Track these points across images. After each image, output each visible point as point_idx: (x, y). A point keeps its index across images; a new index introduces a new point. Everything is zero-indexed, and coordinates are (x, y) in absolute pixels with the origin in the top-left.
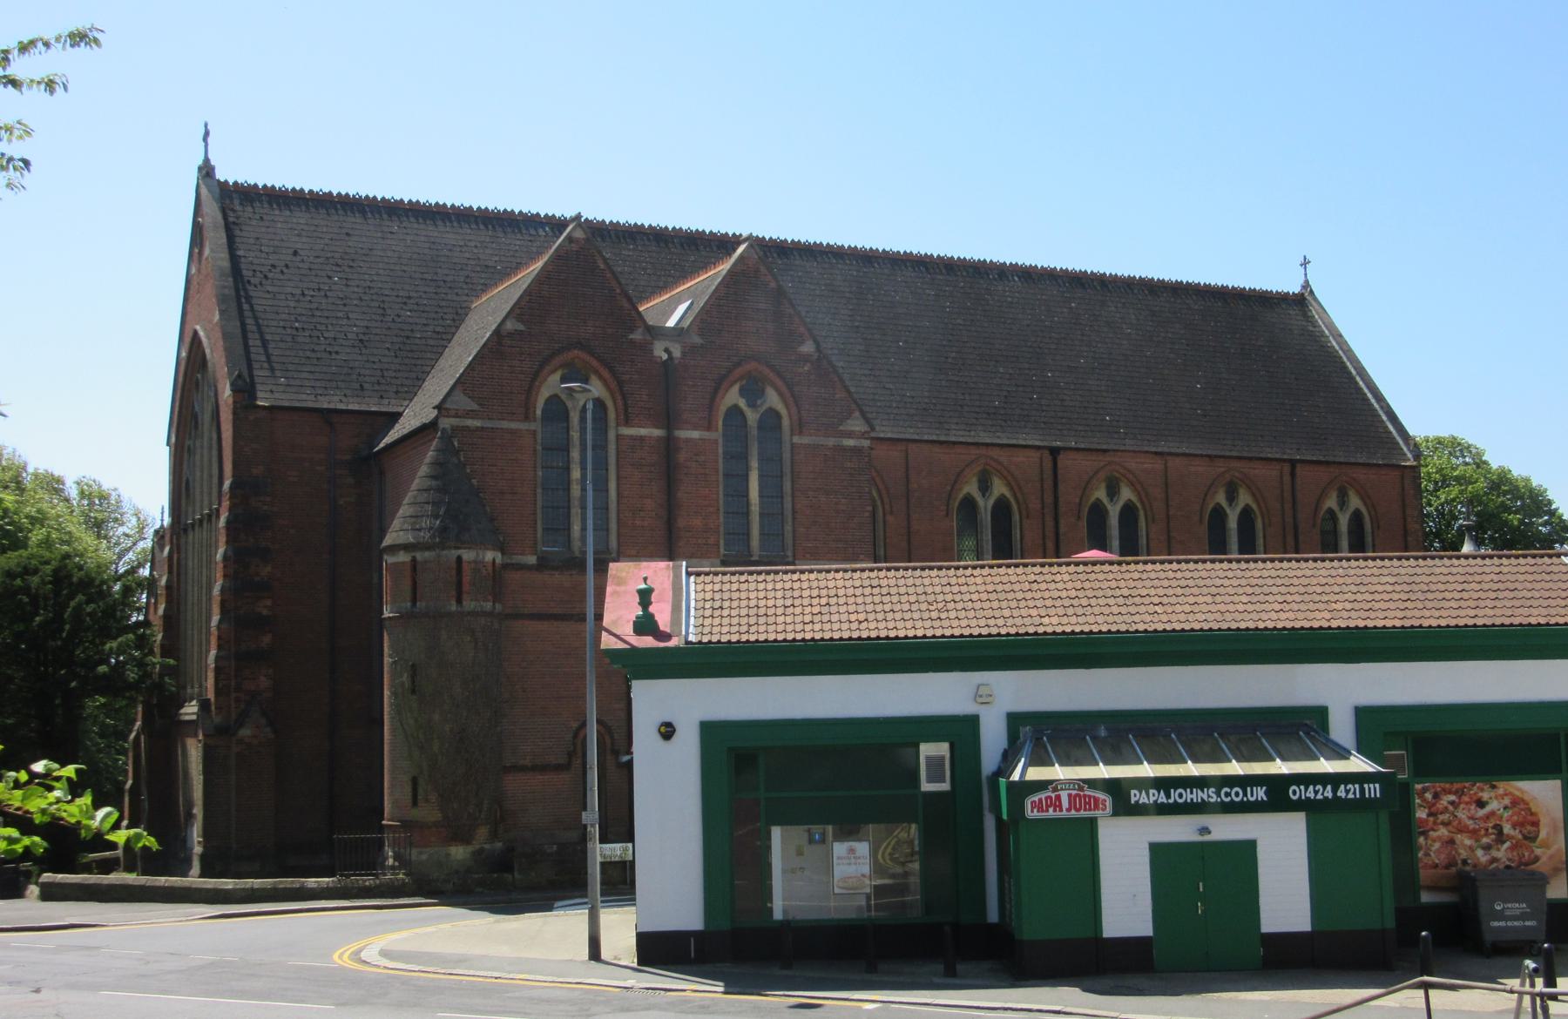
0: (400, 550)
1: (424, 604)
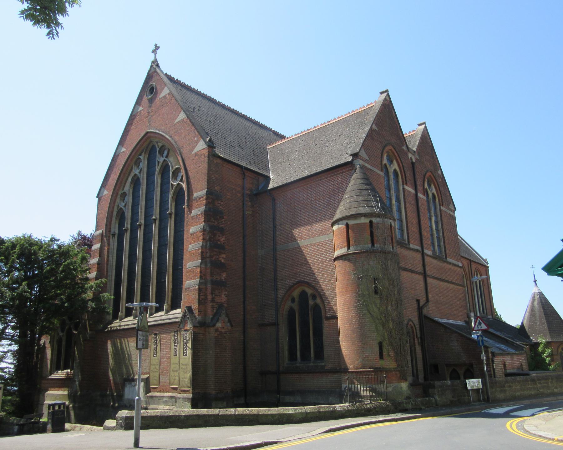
1: (379, 246)
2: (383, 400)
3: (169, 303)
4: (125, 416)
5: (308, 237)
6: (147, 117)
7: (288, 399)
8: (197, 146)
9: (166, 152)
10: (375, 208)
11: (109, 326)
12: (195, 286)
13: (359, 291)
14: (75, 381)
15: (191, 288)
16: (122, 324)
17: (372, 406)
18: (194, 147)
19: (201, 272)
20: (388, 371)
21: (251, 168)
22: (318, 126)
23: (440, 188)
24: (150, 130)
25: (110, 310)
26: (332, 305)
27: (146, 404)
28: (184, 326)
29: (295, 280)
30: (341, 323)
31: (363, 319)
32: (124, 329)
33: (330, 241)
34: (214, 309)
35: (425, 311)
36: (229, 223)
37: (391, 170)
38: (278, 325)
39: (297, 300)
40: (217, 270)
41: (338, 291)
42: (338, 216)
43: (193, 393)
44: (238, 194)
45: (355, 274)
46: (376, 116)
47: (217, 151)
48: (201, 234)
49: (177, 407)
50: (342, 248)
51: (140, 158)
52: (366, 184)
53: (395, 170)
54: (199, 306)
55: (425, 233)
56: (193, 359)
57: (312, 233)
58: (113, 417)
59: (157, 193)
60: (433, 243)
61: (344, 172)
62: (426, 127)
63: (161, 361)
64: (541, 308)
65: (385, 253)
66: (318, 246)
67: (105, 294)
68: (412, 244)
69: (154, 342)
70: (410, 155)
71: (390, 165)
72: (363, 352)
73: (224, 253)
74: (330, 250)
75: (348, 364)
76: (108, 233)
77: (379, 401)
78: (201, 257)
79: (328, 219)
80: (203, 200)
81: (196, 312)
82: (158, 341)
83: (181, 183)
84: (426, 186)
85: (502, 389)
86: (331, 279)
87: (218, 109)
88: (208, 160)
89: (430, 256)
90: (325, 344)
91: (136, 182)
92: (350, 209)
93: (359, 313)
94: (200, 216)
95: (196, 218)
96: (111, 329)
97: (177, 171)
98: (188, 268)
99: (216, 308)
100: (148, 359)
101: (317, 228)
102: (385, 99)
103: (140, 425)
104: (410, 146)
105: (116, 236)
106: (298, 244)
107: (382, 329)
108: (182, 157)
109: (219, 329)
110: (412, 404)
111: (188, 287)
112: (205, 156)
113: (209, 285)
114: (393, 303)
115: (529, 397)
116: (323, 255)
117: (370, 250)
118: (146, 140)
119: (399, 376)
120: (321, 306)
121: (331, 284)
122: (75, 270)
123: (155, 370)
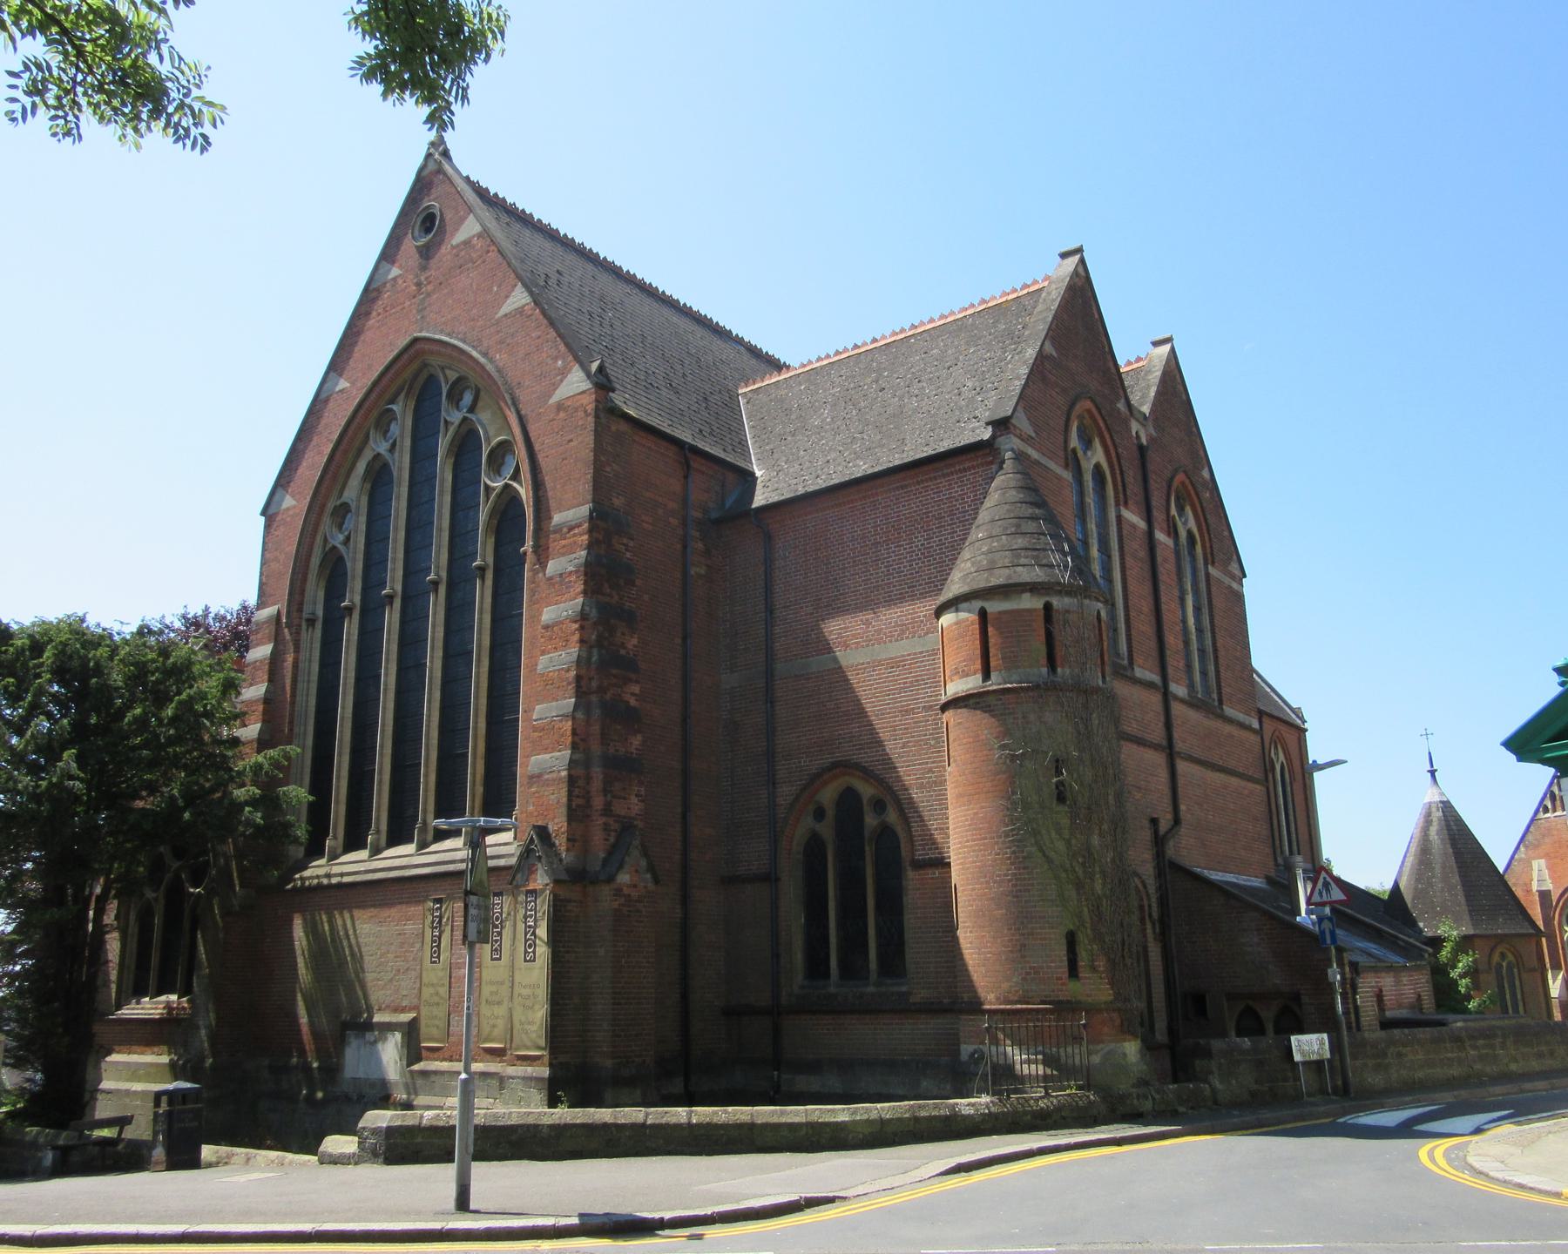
0: (1023, 591)
1: (1068, 671)
2: (1080, 1088)
4: (385, 1125)
6: (414, 297)
7: (803, 1082)
8: (564, 383)
9: (468, 398)
10: (1060, 571)
11: (297, 876)
13: (1014, 793)
14: (198, 1028)
15: (546, 777)
16: (336, 870)
17: (1052, 1103)
18: (555, 386)
19: (574, 733)
20: (1091, 1010)
21: (706, 449)
22: (884, 337)
23: (1208, 517)
24: (424, 334)
25: (301, 832)
26: (930, 830)
27: (409, 1094)
28: (527, 880)
30: (963, 880)
31: (1024, 868)
32: (340, 886)
33: (929, 656)
34: (609, 835)
35: (1170, 851)
36: (646, 597)
37: (1088, 467)
38: (777, 880)
39: (830, 813)
40: (619, 727)
41: (951, 792)
42: (955, 586)
43: (551, 1065)
44: (671, 519)
45: (1003, 747)
46: (1053, 318)
47: (618, 399)
48: (576, 626)
49: (506, 1103)
50: (967, 675)
51: (391, 410)
52: (1031, 503)
53: (1097, 467)
54: (569, 824)
55: (1173, 640)
56: (553, 972)
58: (348, 1128)
59: (441, 507)
60: (1189, 667)
61: (969, 469)
62: (1173, 350)
63: (453, 975)
65: (1085, 692)
67: (291, 787)
68: (1139, 666)
69: (433, 922)
70: (1135, 426)
71: (1085, 453)
73: (637, 682)
75: (980, 990)
76: (295, 614)
77: (1068, 1092)
78: (573, 691)
79: (921, 594)
80: (581, 535)
81: (561, 842)
82: (444, 920)
83: (515, 485)
84: (1173, 511)
85: (1379, 1061)
87: (605, 279)
88: (595, 423)
89: (1182, 701)
90: (908, 935)
91: (379, 476)
92: (990, 569)
93: (1014, 852)
94: (573, 578)
96: (303, 884)
97: (504, 449)
99: (616, 831)
100: (415, 970)
102: (1075, 273)
103: (471, 1149)
104: (1135, 399)
105: (319, 625)
106: (835, 660)
108: (518, 412)
109: (625, 888)
110: (1154, 1099)
111: (536, 771)
112: (585, 411)
113: (598, 769)
114: (1105, 827)
115: (1449, 1084)
116: (906, 692)
117: (1044, 683)
118: (411, 361)
119: (1118, 1022)
120: (902, 834)
121: (930, 771)
122: (208, 714)
123: (436, 999)
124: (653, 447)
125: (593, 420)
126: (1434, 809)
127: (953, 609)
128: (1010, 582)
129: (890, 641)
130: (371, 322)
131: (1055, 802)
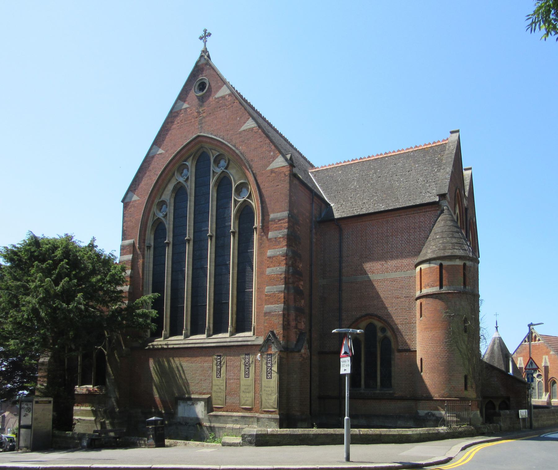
0: (457, 258)
1: (469, 288)
2: (468, 425)
3: (233, 325)
5: (381, 271)
12: (279, 312)
15: (272, 313)
18: (270, 163)
26: (405, 339)
28: (267, 350)
29: (364, 312)
31: (452, 354)
33: (408, 278)
45: (446, 313)
48: (284, 258)
50: (433, 287)
54: (283, 331)
57: (386, 268)
61: (428, 211)
64: (500, 352)
66: (392, 282)
72: (450, 383)
74: (407, 287)
78: (284, 282)
79: (405, 256)
80: (284, 223)
81: (280, 337)
83: (249, 200)
86: (406, 314)
93: (448, 348)
95: (276, 241)
98: (266, 292)
101: (393, 264)
106: (368, 277)
107: (468, 364)
110: (488, 428)
111: (268, 311)
112: (285, 174)
113: (292, 312)
121: (406, 319)
124: (303, 191)
125: (289, 178)
126: (496, 340)
127: (428, 262)
128: (453, 254)
129: (392, 272)
130: (174, 126)
131: (464, 332)
